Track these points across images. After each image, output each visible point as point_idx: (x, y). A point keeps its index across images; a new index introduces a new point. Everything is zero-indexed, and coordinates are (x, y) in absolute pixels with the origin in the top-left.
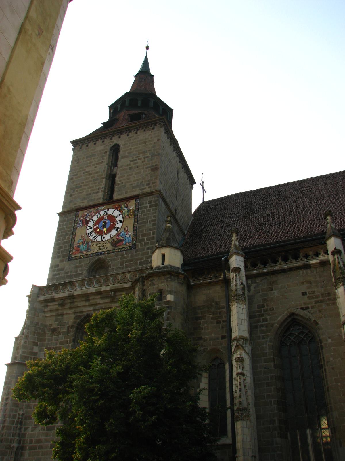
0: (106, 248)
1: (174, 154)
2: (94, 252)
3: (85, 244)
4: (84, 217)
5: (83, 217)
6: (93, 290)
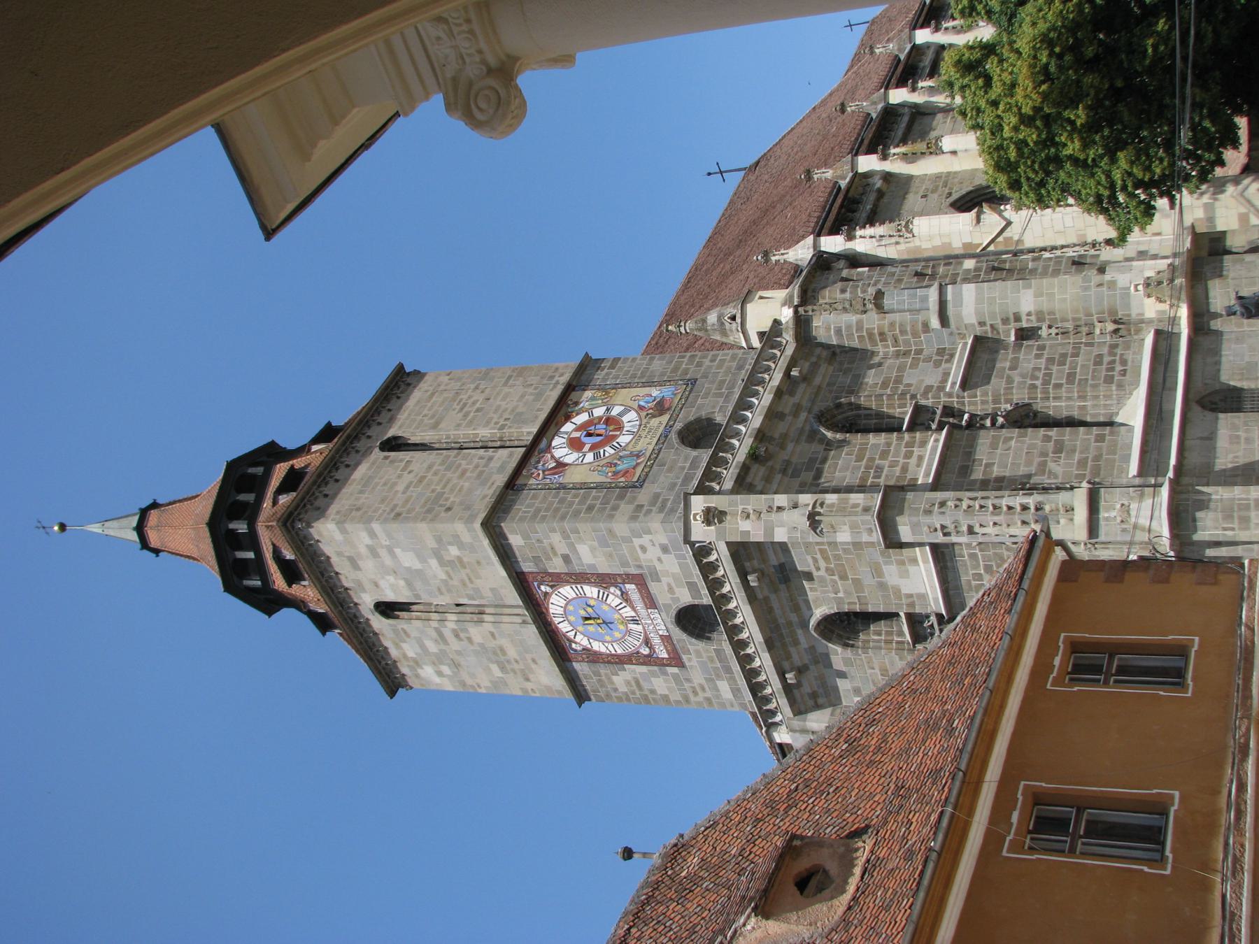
0: (660, 423)
3: (619, 463)
4: (541, 472)
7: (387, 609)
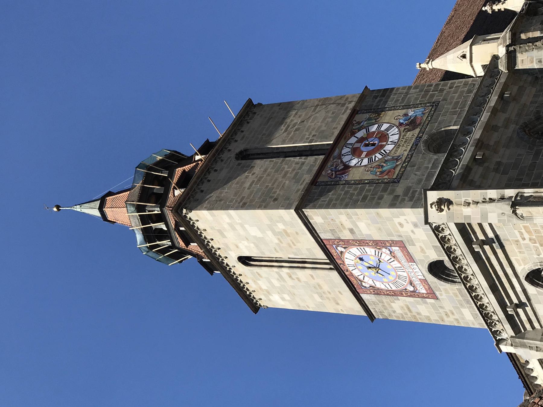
3: (384, 165)
4: (334, 173)
7: (245, 260)
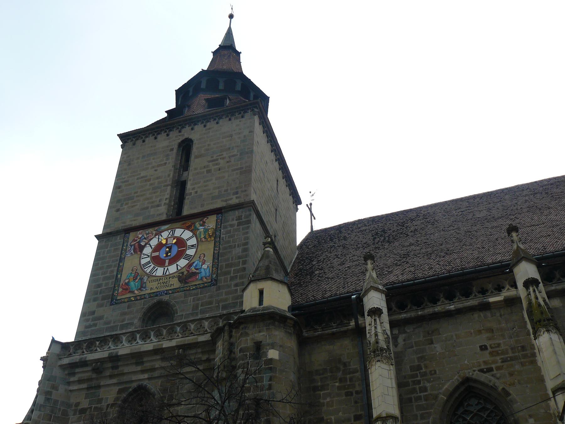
1: (272, 156)
2: (152, 291)
3: (137, 280)
5: (134, 240)
6: (149, 347)
